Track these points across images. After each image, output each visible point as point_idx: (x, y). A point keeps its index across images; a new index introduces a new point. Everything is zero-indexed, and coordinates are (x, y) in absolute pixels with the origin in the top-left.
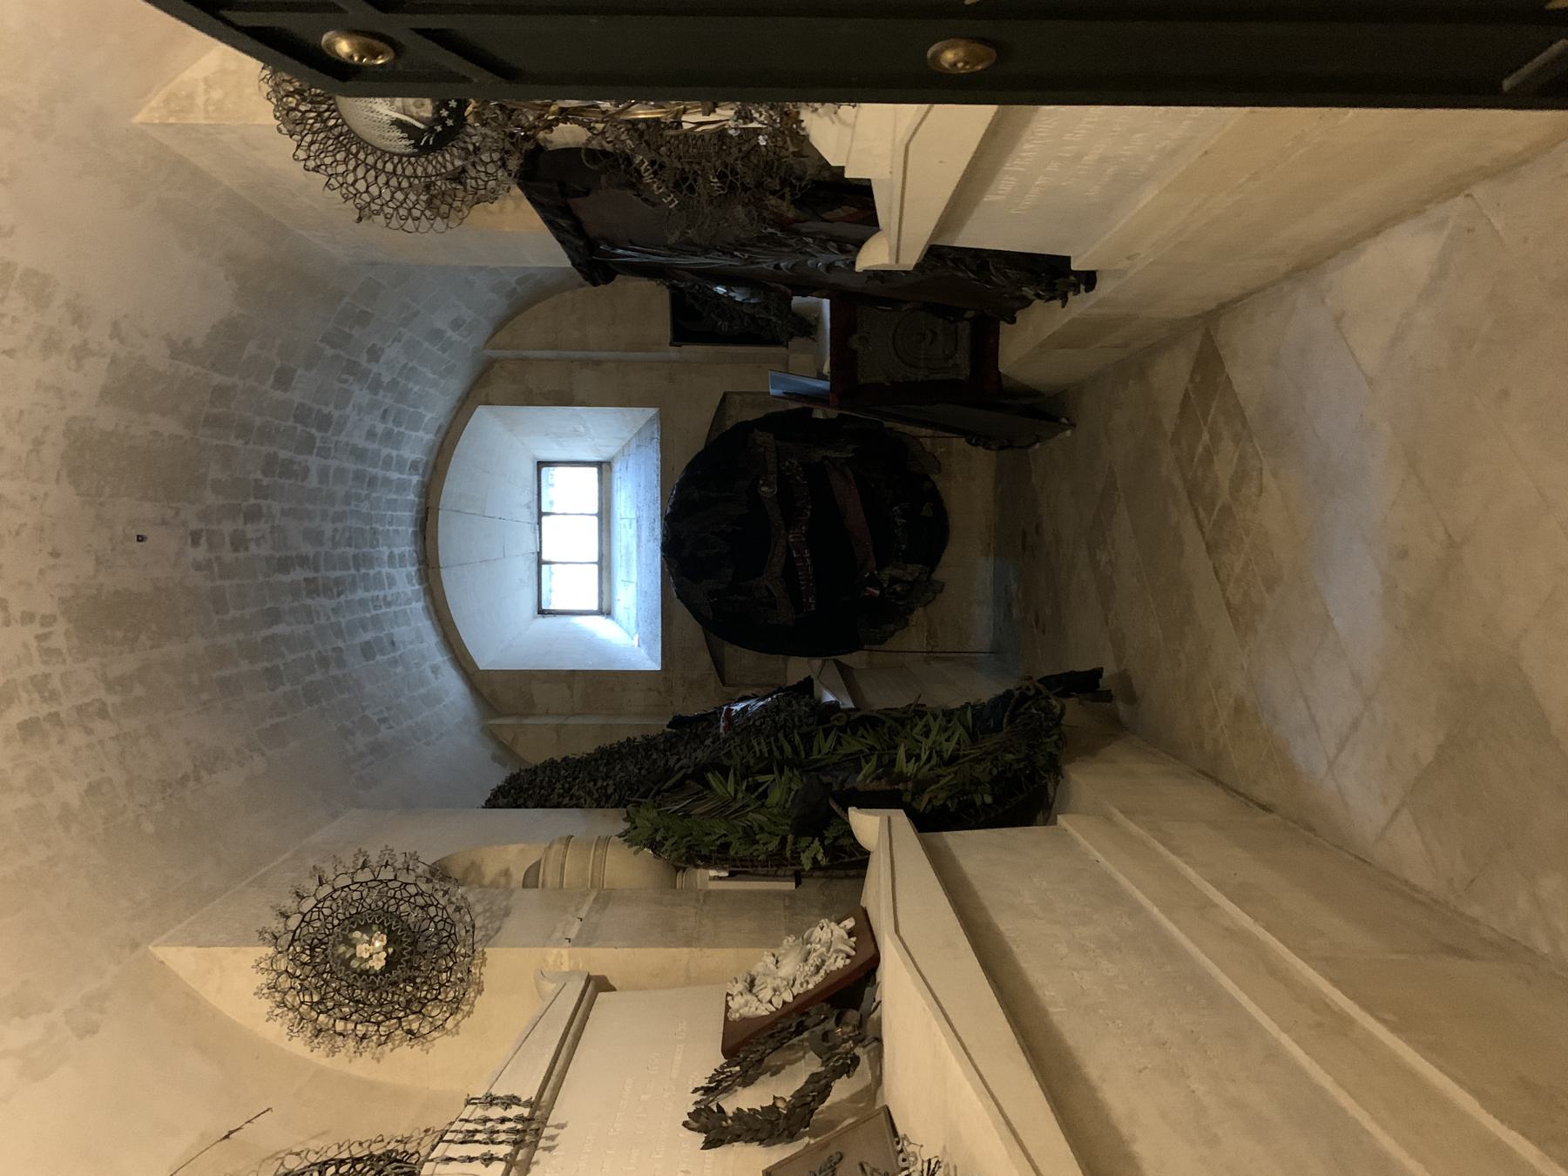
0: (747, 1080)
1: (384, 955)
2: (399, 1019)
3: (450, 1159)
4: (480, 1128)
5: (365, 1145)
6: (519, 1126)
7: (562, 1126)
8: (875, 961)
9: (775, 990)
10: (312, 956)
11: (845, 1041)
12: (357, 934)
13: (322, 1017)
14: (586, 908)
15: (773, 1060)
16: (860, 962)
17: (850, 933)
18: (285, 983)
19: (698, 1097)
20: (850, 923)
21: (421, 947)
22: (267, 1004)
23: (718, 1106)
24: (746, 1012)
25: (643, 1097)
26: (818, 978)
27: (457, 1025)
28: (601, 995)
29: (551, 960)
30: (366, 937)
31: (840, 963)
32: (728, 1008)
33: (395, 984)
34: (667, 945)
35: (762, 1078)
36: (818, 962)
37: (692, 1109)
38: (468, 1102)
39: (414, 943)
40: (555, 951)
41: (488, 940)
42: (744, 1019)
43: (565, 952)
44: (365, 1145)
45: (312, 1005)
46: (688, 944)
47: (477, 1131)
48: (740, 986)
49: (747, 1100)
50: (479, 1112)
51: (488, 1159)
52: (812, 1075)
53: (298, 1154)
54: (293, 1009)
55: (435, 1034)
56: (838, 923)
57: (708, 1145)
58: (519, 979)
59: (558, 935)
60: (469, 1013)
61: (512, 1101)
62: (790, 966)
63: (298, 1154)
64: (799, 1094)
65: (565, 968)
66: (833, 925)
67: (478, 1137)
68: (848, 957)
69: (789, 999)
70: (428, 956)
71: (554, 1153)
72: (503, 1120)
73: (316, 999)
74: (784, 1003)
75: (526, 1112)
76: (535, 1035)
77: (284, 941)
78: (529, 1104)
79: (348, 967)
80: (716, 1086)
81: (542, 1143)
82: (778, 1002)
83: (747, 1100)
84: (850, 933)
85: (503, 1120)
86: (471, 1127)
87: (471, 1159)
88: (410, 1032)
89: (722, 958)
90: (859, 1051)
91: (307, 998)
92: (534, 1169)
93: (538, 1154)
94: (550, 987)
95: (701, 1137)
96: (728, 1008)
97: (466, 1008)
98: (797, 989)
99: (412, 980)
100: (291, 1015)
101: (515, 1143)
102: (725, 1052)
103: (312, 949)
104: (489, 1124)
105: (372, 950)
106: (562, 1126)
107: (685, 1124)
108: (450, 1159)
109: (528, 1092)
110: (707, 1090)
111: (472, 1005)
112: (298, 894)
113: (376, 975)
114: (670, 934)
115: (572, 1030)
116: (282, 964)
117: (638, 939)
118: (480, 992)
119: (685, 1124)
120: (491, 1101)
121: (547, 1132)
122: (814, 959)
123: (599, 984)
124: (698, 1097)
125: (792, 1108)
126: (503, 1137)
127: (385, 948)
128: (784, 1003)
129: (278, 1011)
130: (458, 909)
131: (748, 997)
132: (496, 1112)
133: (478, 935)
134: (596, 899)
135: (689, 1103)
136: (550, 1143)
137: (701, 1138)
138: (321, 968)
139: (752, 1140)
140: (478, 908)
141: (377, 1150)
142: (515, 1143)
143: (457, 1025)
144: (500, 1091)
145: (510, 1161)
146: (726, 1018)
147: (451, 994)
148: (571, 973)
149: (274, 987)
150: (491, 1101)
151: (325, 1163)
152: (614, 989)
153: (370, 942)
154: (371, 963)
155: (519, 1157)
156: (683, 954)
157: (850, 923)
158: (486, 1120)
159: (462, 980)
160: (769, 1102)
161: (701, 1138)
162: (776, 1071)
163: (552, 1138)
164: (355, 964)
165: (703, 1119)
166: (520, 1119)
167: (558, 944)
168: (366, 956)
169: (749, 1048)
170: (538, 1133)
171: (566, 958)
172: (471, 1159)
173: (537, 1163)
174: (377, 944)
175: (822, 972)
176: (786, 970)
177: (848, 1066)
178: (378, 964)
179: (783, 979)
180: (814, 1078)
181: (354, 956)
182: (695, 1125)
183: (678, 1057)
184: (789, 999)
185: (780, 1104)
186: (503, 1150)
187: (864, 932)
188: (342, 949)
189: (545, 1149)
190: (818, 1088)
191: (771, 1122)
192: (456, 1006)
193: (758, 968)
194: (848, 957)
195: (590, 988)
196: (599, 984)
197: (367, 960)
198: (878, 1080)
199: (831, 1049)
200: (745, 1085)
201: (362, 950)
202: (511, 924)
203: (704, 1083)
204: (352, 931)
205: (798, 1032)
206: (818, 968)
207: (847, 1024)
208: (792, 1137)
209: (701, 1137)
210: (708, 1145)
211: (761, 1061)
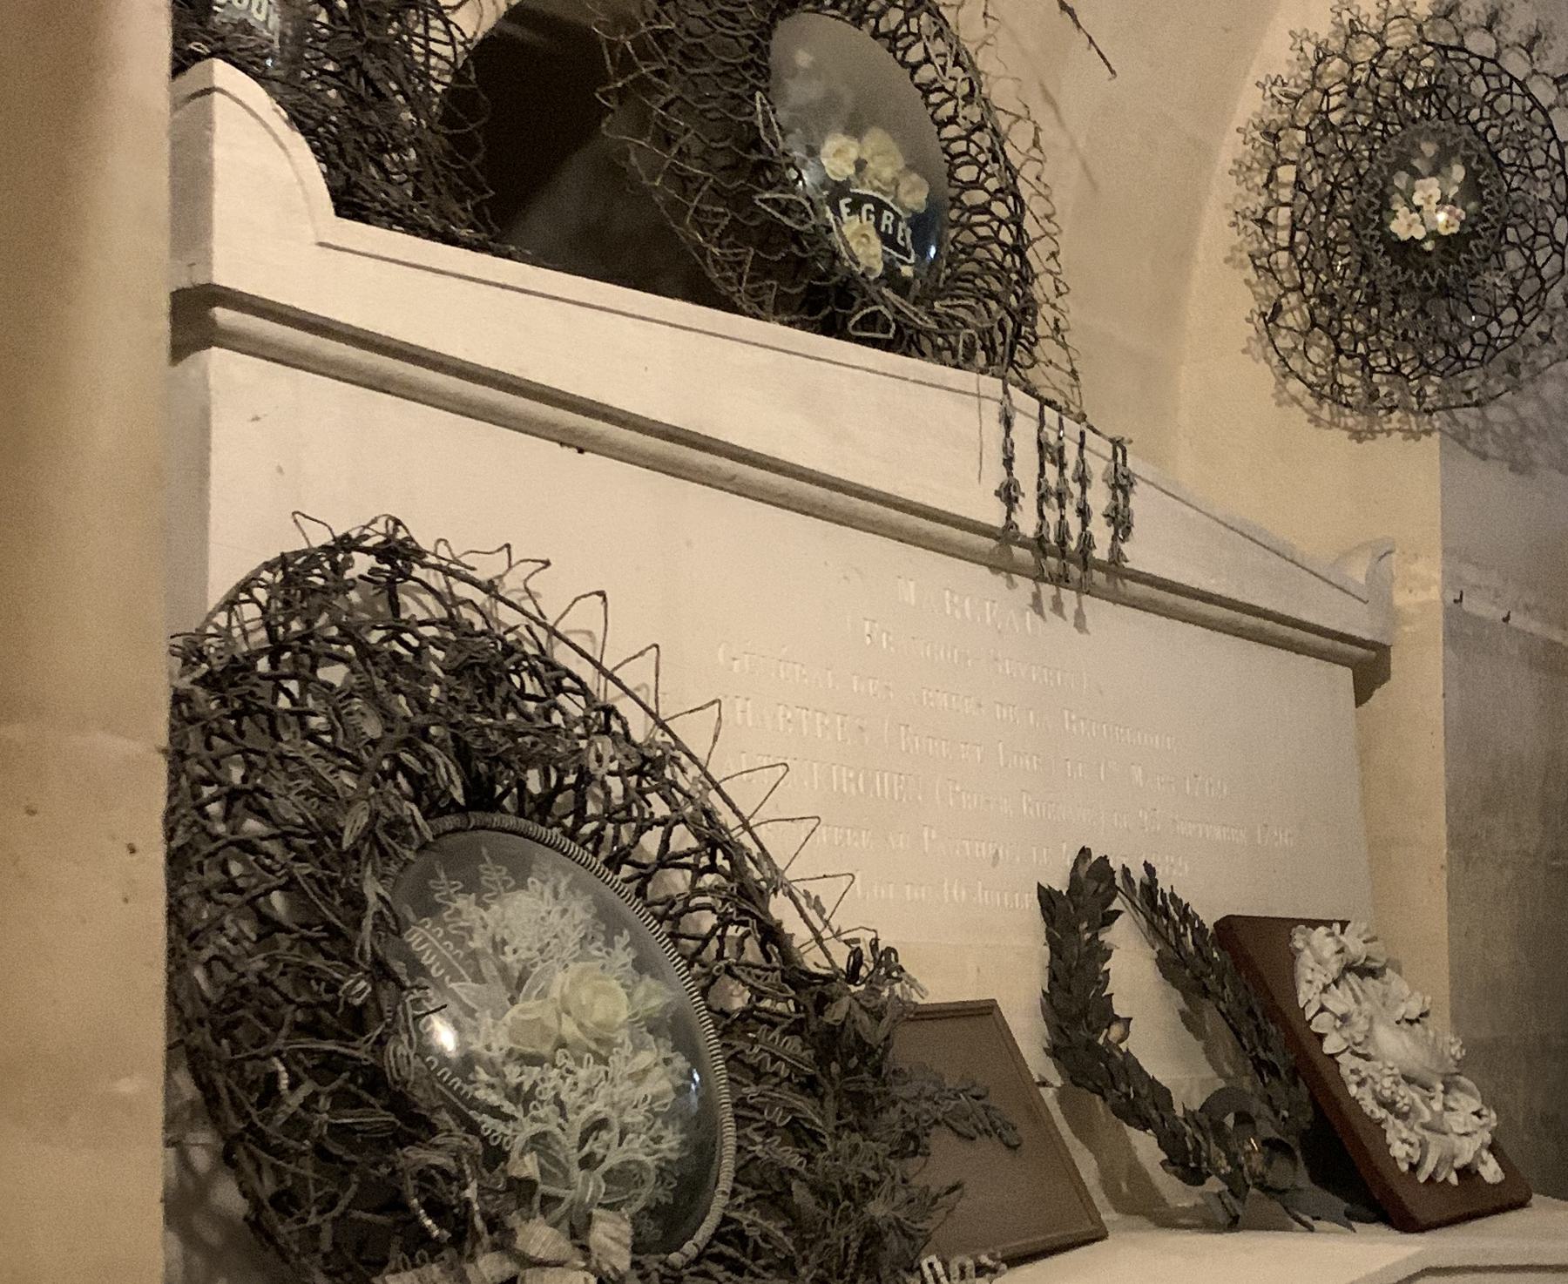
0: (1172, 966)
1: (1420, 234)
2: (1302, 287)
3: (1007, 422)
4: (1068, 473)
5: (1052, 265)
6: (1073, 545)
7: (1080, 623)
8: (1406, 1223)
9: (1344, 1018)
10: (1411, 95)
11: (1232, 1159)
12: (1458, 172)
13: (1301, 136)
14: (1534, 626)
15: (1212, 1019)
16: (1401, 1190)
17: (1468, 1173)
18: (1364, 50)
19: (1138, 874)
20: (1491, 1171)
21: (1439, 309)
22: (1323, 28)
23: (1119, 913)
24: (1306, 960)
25: (1138, 773)
26: (1369, 1105)
27: (1295, 400)
28: (1345, 675)
29: (1419, 568)
30: (1453, 191)
31: (1399, 1150)
32: (1314, 924)
33: (1365, 266)
34: (1452, 798)
35: (1177, 996)
36: (1401, 1105)
37: (1115, 864)
38: (1116, 443)
39: (1445, 291)
40: (1438, 576)
41: (1460, 437)
42: (1293, 955)
43: (1434, 593)
44: (1052, 265)
45: (1322, 114)
46: (1454, 840)
47: (1063, 466)
48: (1356, 947)
49: (1130, 967)
50: (1098, 467)
51: (1009, 494)
52: (1167, 1092)
53: (1036, 144)
54: (1316, 76)
55: (1275, 359)
56: (1492, 1148)
57: (1047, 897)
58: (1381, 511)
59: (1471, 575)
60: (1315, 420)
61: (1121, 522)
62: (1394, 1045)
63: (1036, 144)
64: (1131, 1067)
65: (1401, 599)
66: (1487, 1138)
67: (1051, 471)
68: (1414, 1168)
69: (1329, 1047)
70: (1422, 324)
71: (1030, 615)
72: (1083, 512)
73: (1335, 118)
74: (1321, 1037)
75: (1101, 553)
76: (1255, 555)
77: (1443, 33)
78: (1116, 556)
79: (1394, 168)
80: (1159, 909)
81: (1048, 590)
82: (1321, 1024)
83: (1130, 967)
84: (1468, 1173)
85: (1083, 512)
86: (1071, 455)
87: (1008, 462)
88: (1277, 309)
89: (1425, 916)
90: (1214, 1185)
91: (1335, 101)
92: (1000, 579)
93: (1025, 586)
94: (1358, 573)
95: (1060, 884)
96: (1314, 924)
97: (1325, 414)
98: (1347, 1062)
99: (1373, 300)
100: (1307, 74)
101: (1041, 539)
102: (1227, 925)
103: (1429, 91)
104: (1075, 488)
105: (1428, 209)
106: (1080, 623)
107: (1085, 852)
108: (1007, 422)
109: (1138, 555)
110: (1150, 888)
111: (1332, 424)
112: (1537, 37)
113: (1382, 225)
114: (1476, 804)
115: (1268, 624)
116: (1398, 37)
117: (1465, 737)
118: (1357, 435)
119: (1085, 852)
120: (1121, 484)
121: (1069, 597)
122: (1408, 1096)
123: (1369, 668)
124: (1138, 874)
125: (1106, 1054)
126: (1052, 516)
127: (1433, 235)
128: (1321, 1037)
129: (1310, 49)
130: (1513, 368)
131: (1334, 967)
132: (1099, 498)
133: (1465, 416)
134: (1551, 645)
135: (1124, 856)
136: (1047, 604)
137: (1059, 882)
138: (1390, 116)
139: (1053, 978)
140: (1529, 409)
141: (1042, 288)
142: (1041, 539)
143: (1295, 400)
144: (1140, 503)
145: (1007, 534)
146: (1296, 922)
147: (1346, 380)
148: (1393, 616)
149: (1354, 32)
150: (1121, 484)
151: (1017, 197)
152: (1359, 702)
153: (1443, 201)
154: (1402, 210)
155: (1017, 551)
156: (1435, 828)
157: (1491, 1171)
158: (1083, 480)
159: (1373, 396)
160: (1120, 1008)
161: (1059, 882)
162: (1191, 1021)
163: (1058, 606)
164: (1401, 180)
165: (1093, 885)
166: (1087, 541)
167: (1451, 579)
168: (1417, 200)
169: (1237, 969)
170: (1061, 580)
171: (1422, 597)
172: (1008, 462)
173: (1012, 585)
174: (1442, 217)
175: (1380, 1113)
176: (1391, 1041)
177: (1188, 1168)
178: (1403, 226)
179: (1368, 1036)
180: (1161, 1095)
181: (1415, 174)
182: (1083, 870)
183: (1219, 833)
184: (1329, 1047)
185: (1116, 1031)
186: (1027, 523)
187: (1469, 1201)
188: (1429, 149)
189: (1037, 597)
190: (1141, 1102)
191: (1084, 1013)
192: (1328, 392)
193: (1396, 983)
194: (1414, 1168)
195: (1359, 652)
196: (1369, 668)
197: (1408, 202)
198: (1167, 1220)
199: (1218, 1128)
200: (1162, 963)
201: (1428, 190)
202: (1494, 480)
203: (1163, 885)
204: (1466, 162)
205: (1260, 1065)
206: (1388, 1105)
207: (1269, 1163)
208: (1054, 1052)
209: (1060, 884)
210: (1047, 897)
211: (1206, 992)
